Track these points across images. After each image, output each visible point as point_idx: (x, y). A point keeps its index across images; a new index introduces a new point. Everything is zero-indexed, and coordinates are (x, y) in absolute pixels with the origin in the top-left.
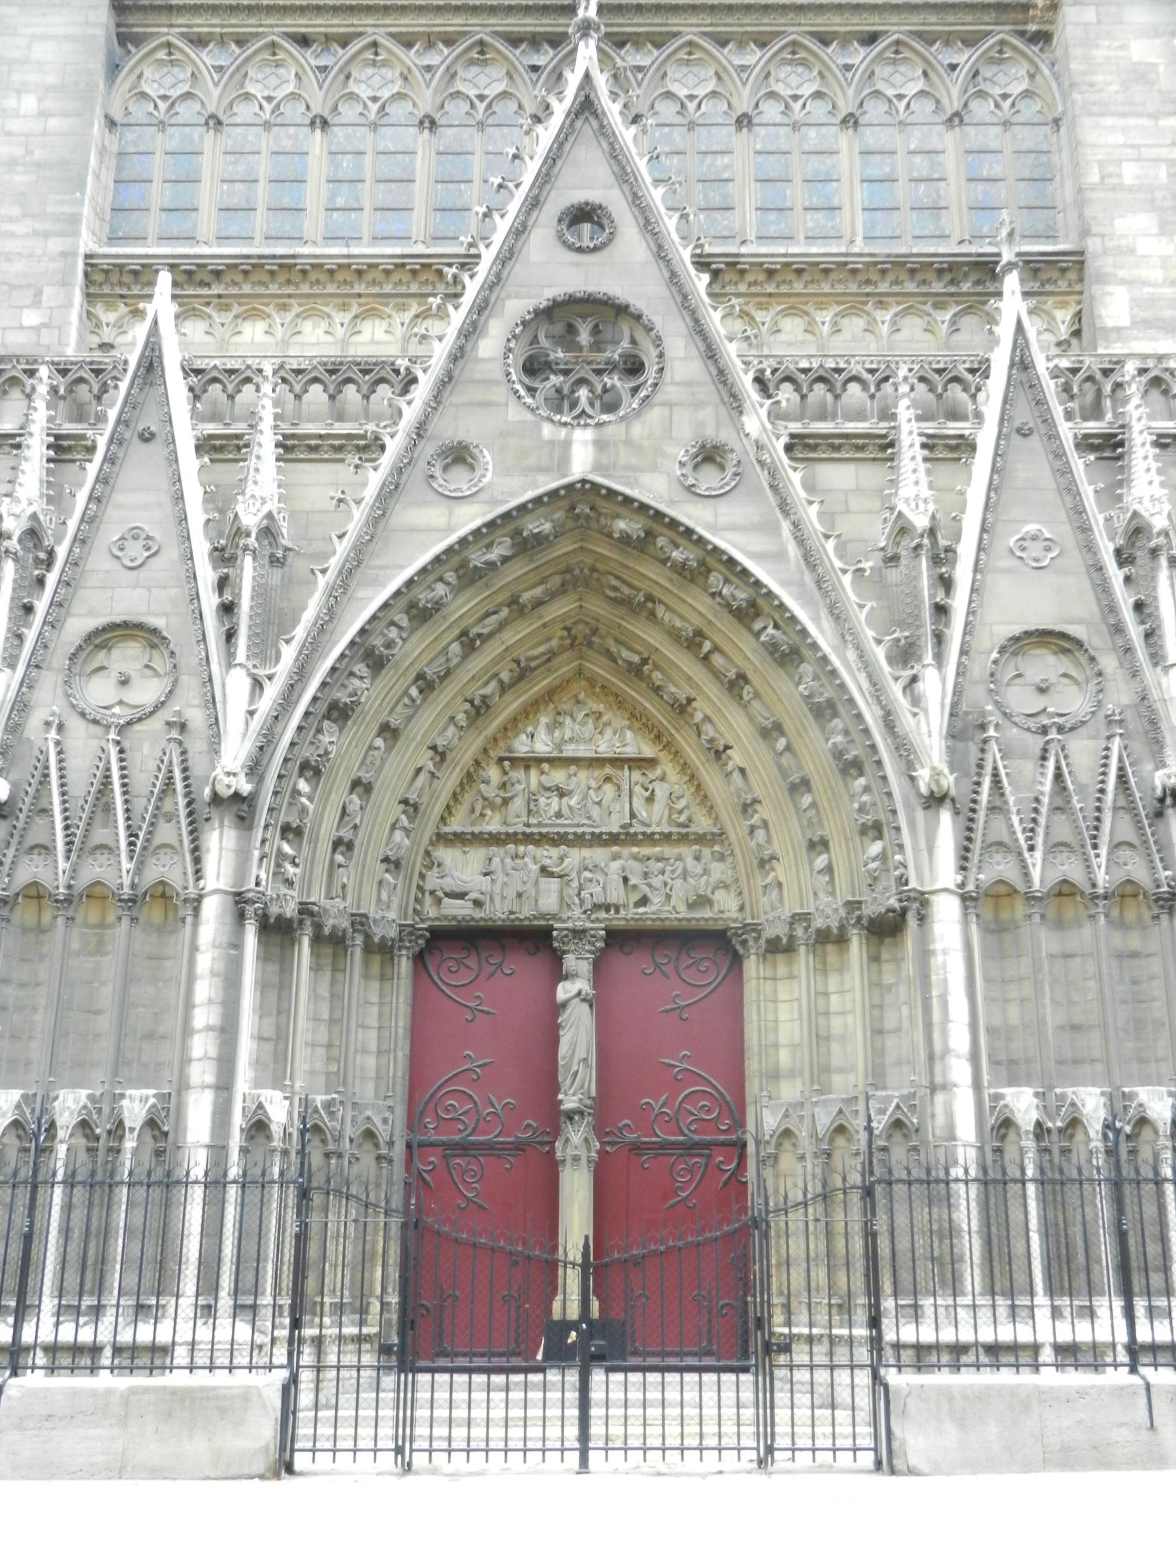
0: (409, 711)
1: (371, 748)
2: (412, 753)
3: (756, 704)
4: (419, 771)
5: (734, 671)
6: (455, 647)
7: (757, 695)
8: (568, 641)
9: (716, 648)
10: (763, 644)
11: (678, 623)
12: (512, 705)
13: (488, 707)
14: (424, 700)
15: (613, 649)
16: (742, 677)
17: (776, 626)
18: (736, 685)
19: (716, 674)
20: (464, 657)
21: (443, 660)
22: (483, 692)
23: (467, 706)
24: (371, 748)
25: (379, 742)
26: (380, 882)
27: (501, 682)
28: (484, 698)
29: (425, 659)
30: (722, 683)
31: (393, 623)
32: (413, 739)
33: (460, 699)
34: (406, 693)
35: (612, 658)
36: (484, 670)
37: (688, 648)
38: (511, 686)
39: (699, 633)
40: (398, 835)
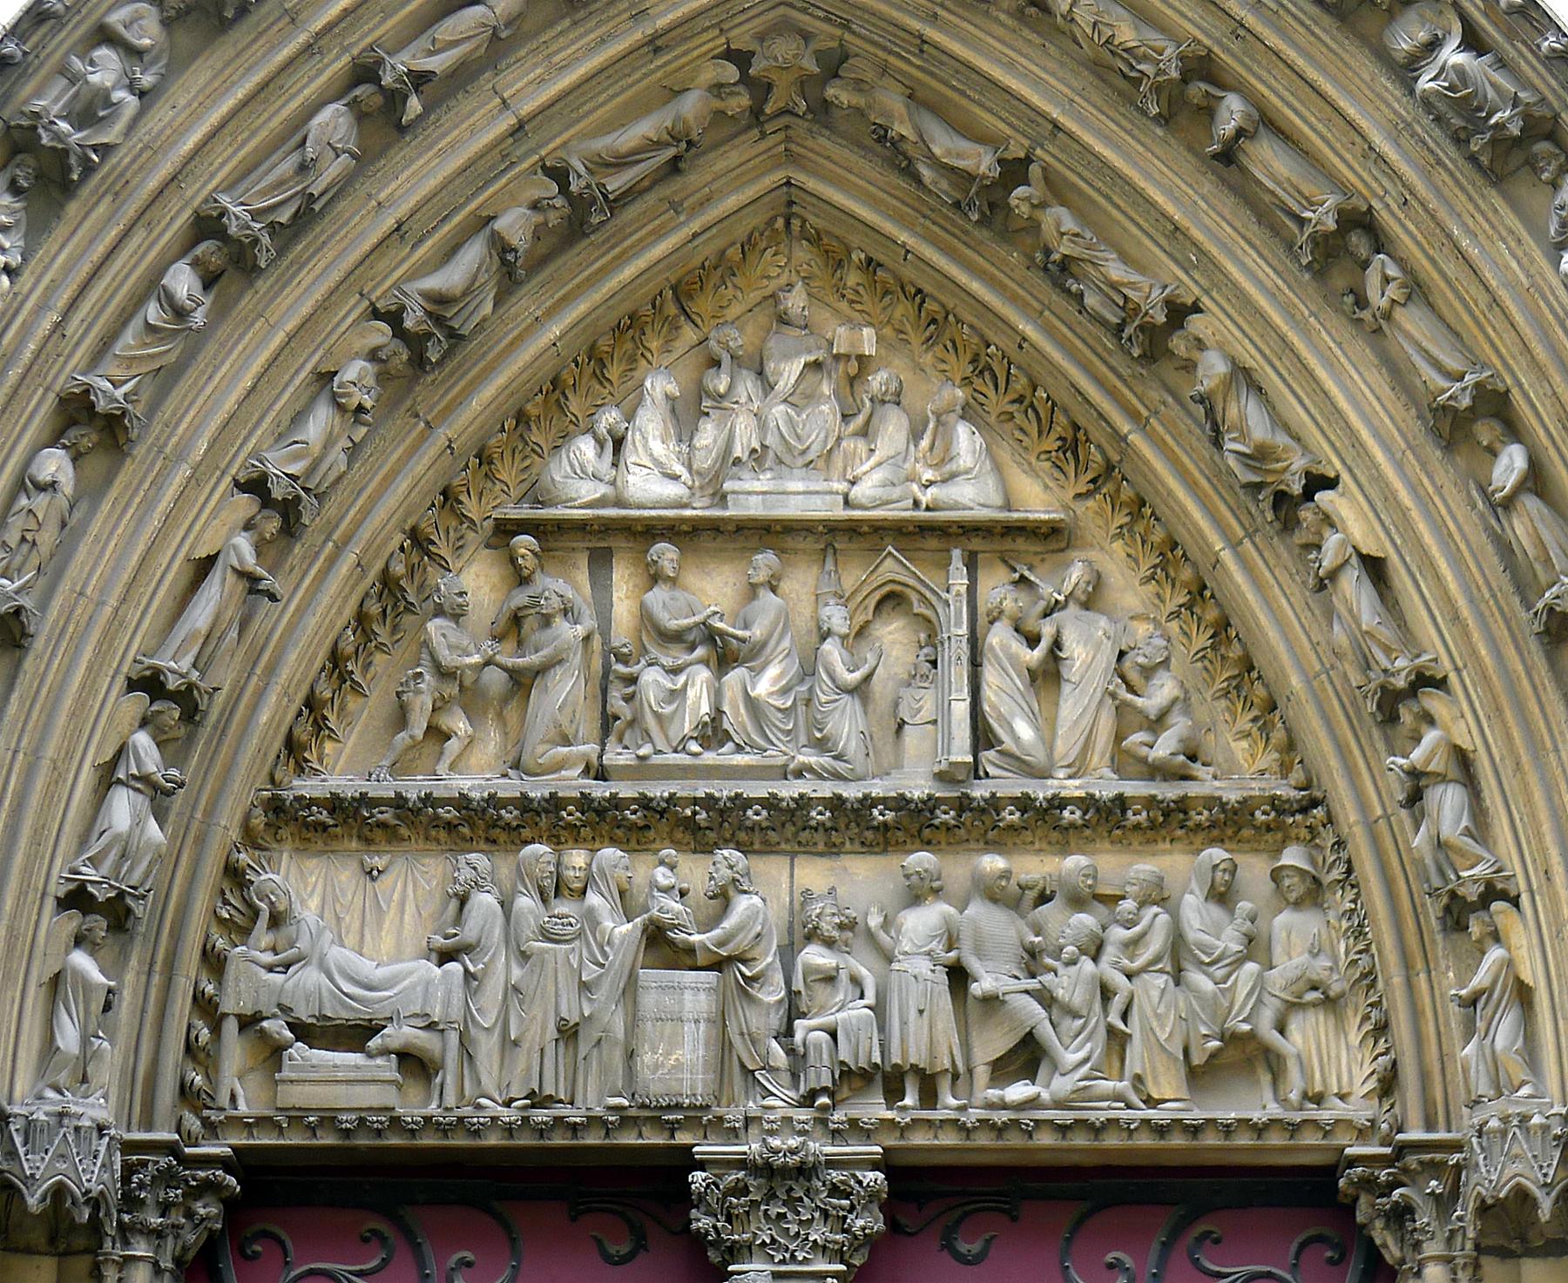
0: (169, 351)
1: (25, 483)
2: (179, 504)
3: (1412, 321)
4: (204, 567)
5: (1331, 201)
6: (333, 121)
7: (1416, 290)
8: (741, 102)
9: (1266, 122)
10: (1426, 102)
11: (1127, 34)
12: (544, 330)
13: (454, 336)
14: (220, 313)
15: (902, 128)
16: (1359, 221)
17: (1473, 41)
18: (1341, 250)
19: (1270, 216)
20: (364, 160)
21: (288, 166)
22: (433, 283)
23: (380, 334)
24: (25, 483)
25: (54, 464)
26: (56, 981)
27: (501, 247)
28: (440, 300)
29: (225, 161)
30: (1290, 246)
31: (105, 36)
32: (180, 456)
33: (353, 308)
34: (153, 286)
35: (899, 158)
36: (438, 205)
37: (1164, 120)
38: (540, 262)
39: (1201, 67)
40: (123, 808)
